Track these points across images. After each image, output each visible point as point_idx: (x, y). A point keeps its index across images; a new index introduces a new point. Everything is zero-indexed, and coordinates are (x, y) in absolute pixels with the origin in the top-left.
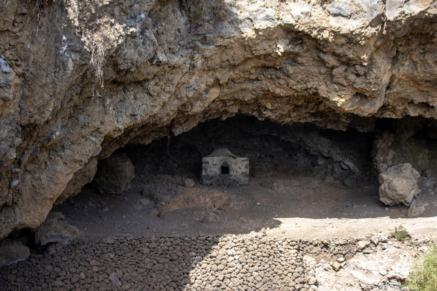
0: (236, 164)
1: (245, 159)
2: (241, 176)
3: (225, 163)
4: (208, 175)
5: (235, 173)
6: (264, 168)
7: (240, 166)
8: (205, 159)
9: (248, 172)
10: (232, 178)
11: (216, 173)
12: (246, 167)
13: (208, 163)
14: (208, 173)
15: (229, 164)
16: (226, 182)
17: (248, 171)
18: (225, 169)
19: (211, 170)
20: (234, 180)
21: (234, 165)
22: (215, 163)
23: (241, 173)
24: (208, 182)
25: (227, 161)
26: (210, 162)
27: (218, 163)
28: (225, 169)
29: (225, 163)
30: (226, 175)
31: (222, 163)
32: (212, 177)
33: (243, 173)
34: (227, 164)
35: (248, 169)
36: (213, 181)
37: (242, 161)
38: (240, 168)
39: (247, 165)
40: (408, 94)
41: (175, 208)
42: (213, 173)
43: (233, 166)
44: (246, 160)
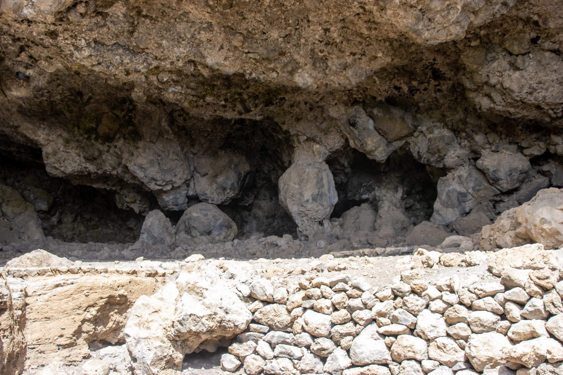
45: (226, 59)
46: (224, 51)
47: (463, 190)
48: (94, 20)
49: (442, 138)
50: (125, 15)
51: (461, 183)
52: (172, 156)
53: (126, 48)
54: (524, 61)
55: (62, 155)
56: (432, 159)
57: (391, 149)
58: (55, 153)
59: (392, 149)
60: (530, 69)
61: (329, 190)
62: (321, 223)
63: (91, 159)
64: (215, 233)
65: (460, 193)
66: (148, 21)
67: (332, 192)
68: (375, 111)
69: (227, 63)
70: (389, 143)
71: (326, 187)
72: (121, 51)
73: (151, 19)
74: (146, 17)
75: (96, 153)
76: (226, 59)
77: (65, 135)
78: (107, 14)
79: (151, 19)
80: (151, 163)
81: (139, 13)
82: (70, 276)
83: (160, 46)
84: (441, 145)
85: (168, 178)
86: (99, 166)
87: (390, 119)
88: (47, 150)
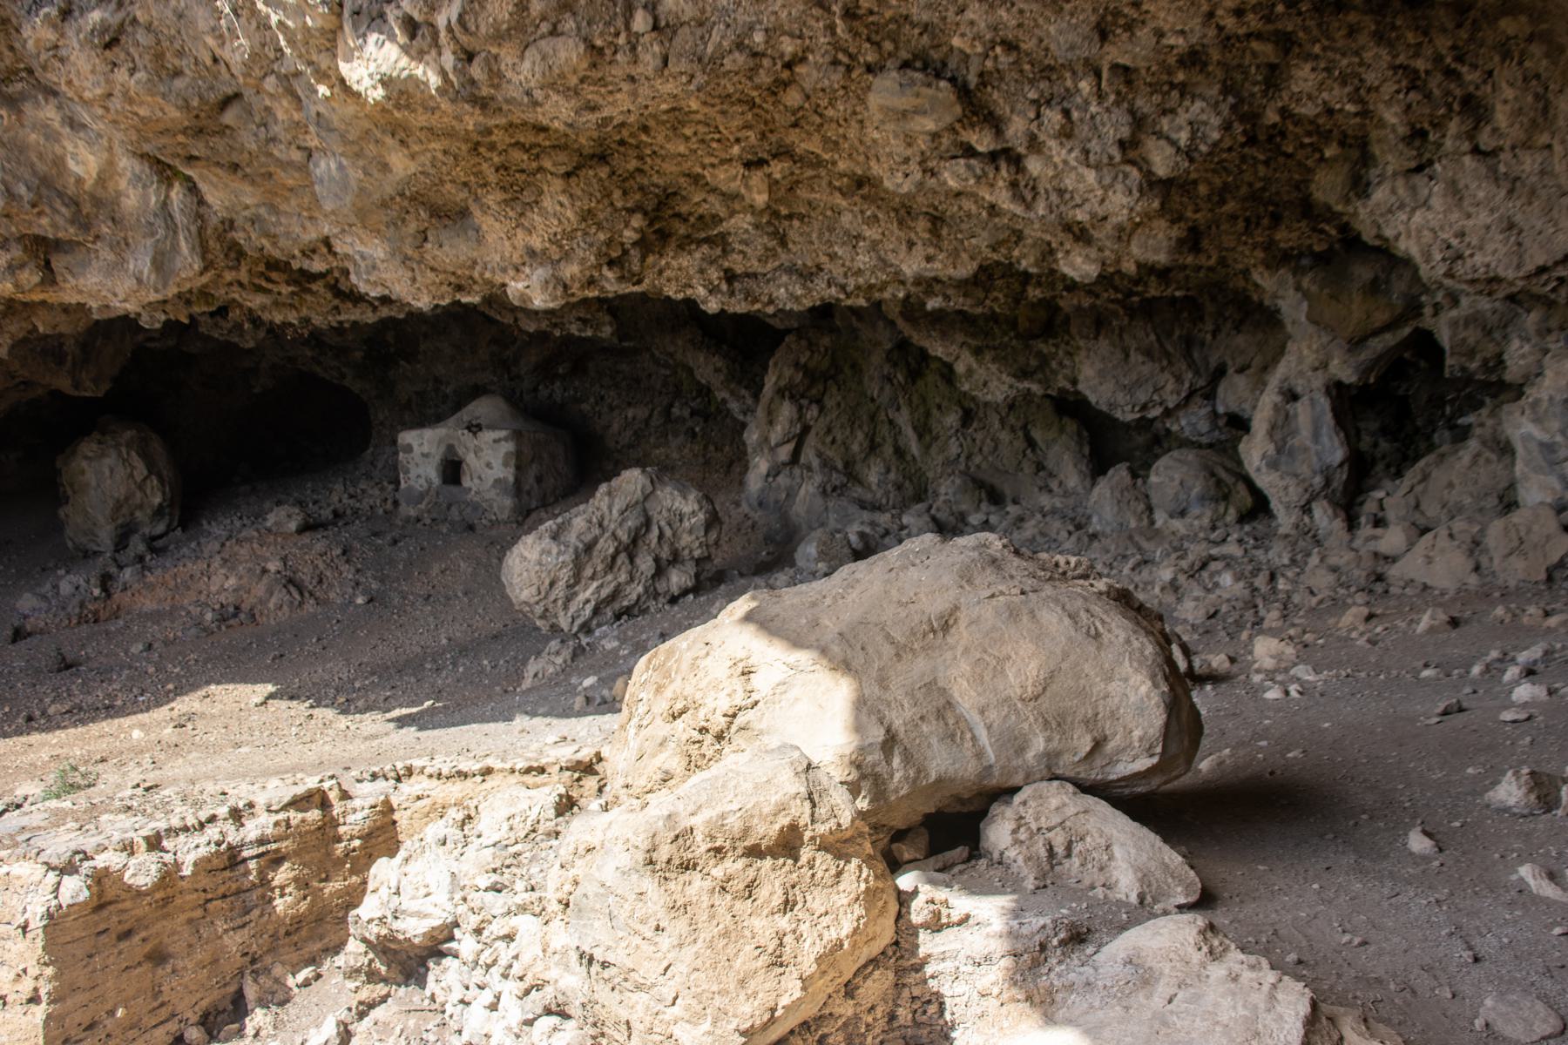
0: (477, 451)
1: (503, 434)
2: (492, 494)
3: (450, 448)
4: (410, 488)
5: (476, 481)
6: (675, 455)
7: (490, 459)
8: (408, 437)
9: (511, 479)
10: (469, 497)
11: (430, 482)
12: (505, 464)
13: (409, 449)
14: (412, 483)
15: (461, 451)
16: (454, 513)
17: (509, 474)
18: (452, 470)
19: (420, 471)
20: (476, 507)
21: (472, 455)
22: (426, 449)
23: (491, 482)
24: (413, 513)
25: (456, 443)
26: (415, 448)
27: (433, 451)
28: (452, 470)
29: (450, 448)
30: (453, 489)
31: (443, 449)
32: (422, 496)
33: (498, 481)
34: (456, 454)
35: (512, 470)
36: (423, 506)
37: (495, 441)
38: (489, 465)
39: (507, 454)
40: (253, 210)
41: (149, 605)
42: (422, 481)
43: (470, 459)
44: (506, 439)
45: (929, 259)
46: (919, 250)
47: (1545, 438)
48: (698, 255)
49: (1473, 320)
50: (757, 226)
51: (1537, 420)
52: (1136, 357)
53: (791, 270)
54: (1413, 190)
55: (981, 374)
56: (1474, 366)
57: (1363, 357)
58: (970, 372)
59: (1365, 355)
60: (1436, 202)
61: (1316, 436)
62: (1306, 509)
63: (1024, 374)
64: (1195, 511)
65: (1542, 445)
66: (796, 223)
67: (1325, 440)
68: (1306, 282)
69: (937, 265)
70: (1356, 343)
71: (1305, 432)
72: (785, 278)
73: (801, 217)
74: (790, 217)
75: (1034, 362)
76: (929, 259)
77: (973, 343)
78: (723, 236)
79: (801, 217)
80: (1101, 374)
81: (776, 214)
82: (435, 782)
83: (832, 257)
84: (1472, 335)
85: (1142, 397)
86: (1045, 383)
87: (1332, 297)
88: (960, 368)
